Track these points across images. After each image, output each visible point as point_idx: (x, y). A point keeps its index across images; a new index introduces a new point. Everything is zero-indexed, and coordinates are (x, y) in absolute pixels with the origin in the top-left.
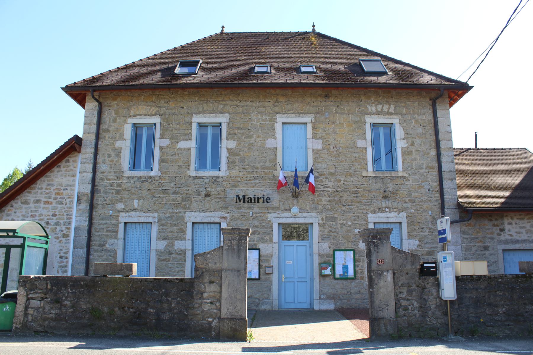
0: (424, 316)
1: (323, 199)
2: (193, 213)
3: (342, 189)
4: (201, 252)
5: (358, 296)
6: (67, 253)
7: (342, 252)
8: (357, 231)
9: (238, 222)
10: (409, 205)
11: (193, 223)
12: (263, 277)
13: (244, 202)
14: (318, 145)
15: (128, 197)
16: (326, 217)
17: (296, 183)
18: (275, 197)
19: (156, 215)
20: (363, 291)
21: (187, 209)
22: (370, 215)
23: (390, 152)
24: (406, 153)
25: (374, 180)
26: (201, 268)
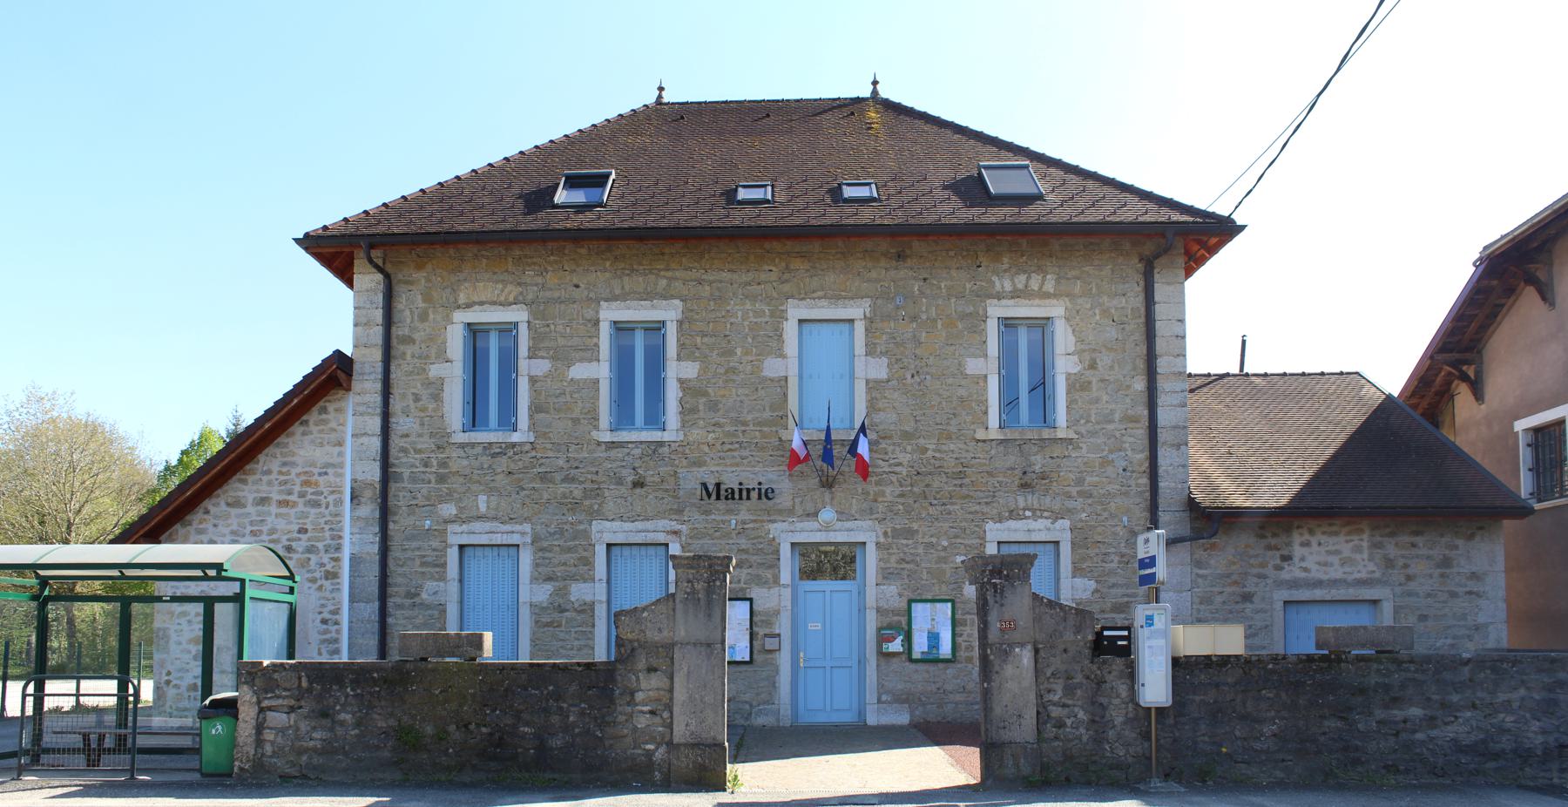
0: (1099, 739)
1: (888, 490)
2: (608, 524)
3: (930, 468)
4: (627, 607)
5: (959, 697)
6: (336, 612)
7: (928, 605)
8: (959, 559)
9: (707, 541)
10: (1078, 504)
11: (609, 545)
12: (758, 657)
13: (718, 498)
14: (878, 369)
15: (463, 489)
16: (894, 530)
17: (827, 456)
18: (784, 486)
19: (527, 527)
20: (971, 686)
22: (990, 526)
23: (1041, 386)
24: (1077, 385)
25: (1001, 448)
26: (631, 641)
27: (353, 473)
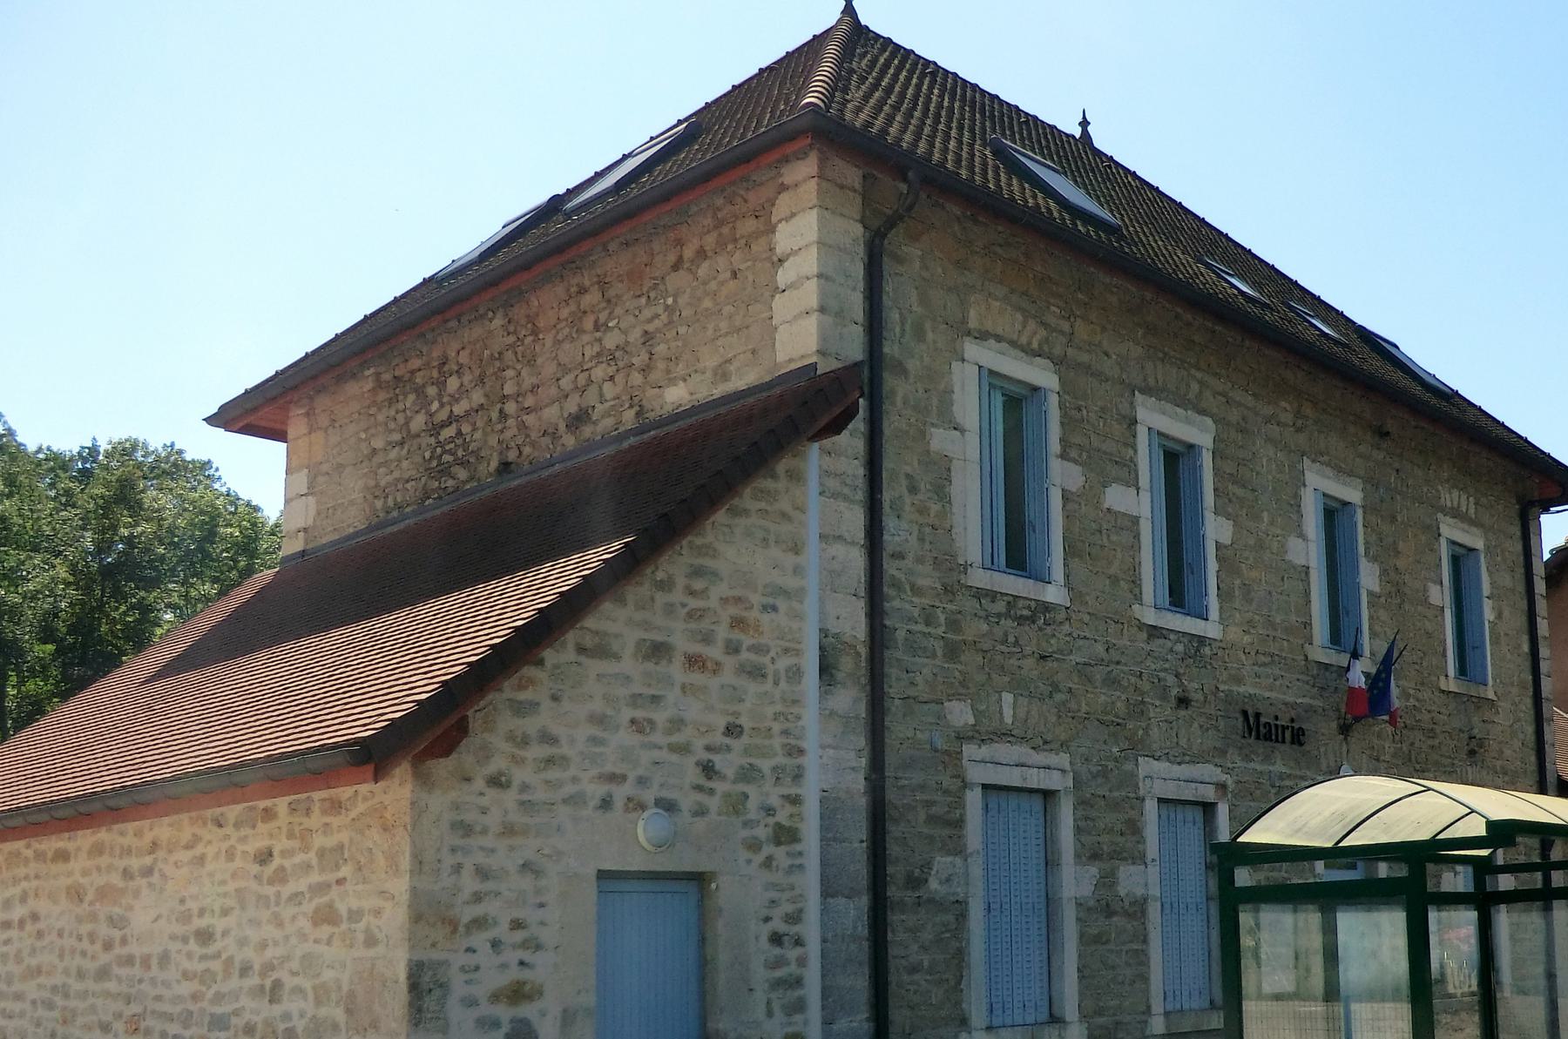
6: (795, 918)
19: (1063, 760)
21: (1137, 748)
27: (823, 614)
